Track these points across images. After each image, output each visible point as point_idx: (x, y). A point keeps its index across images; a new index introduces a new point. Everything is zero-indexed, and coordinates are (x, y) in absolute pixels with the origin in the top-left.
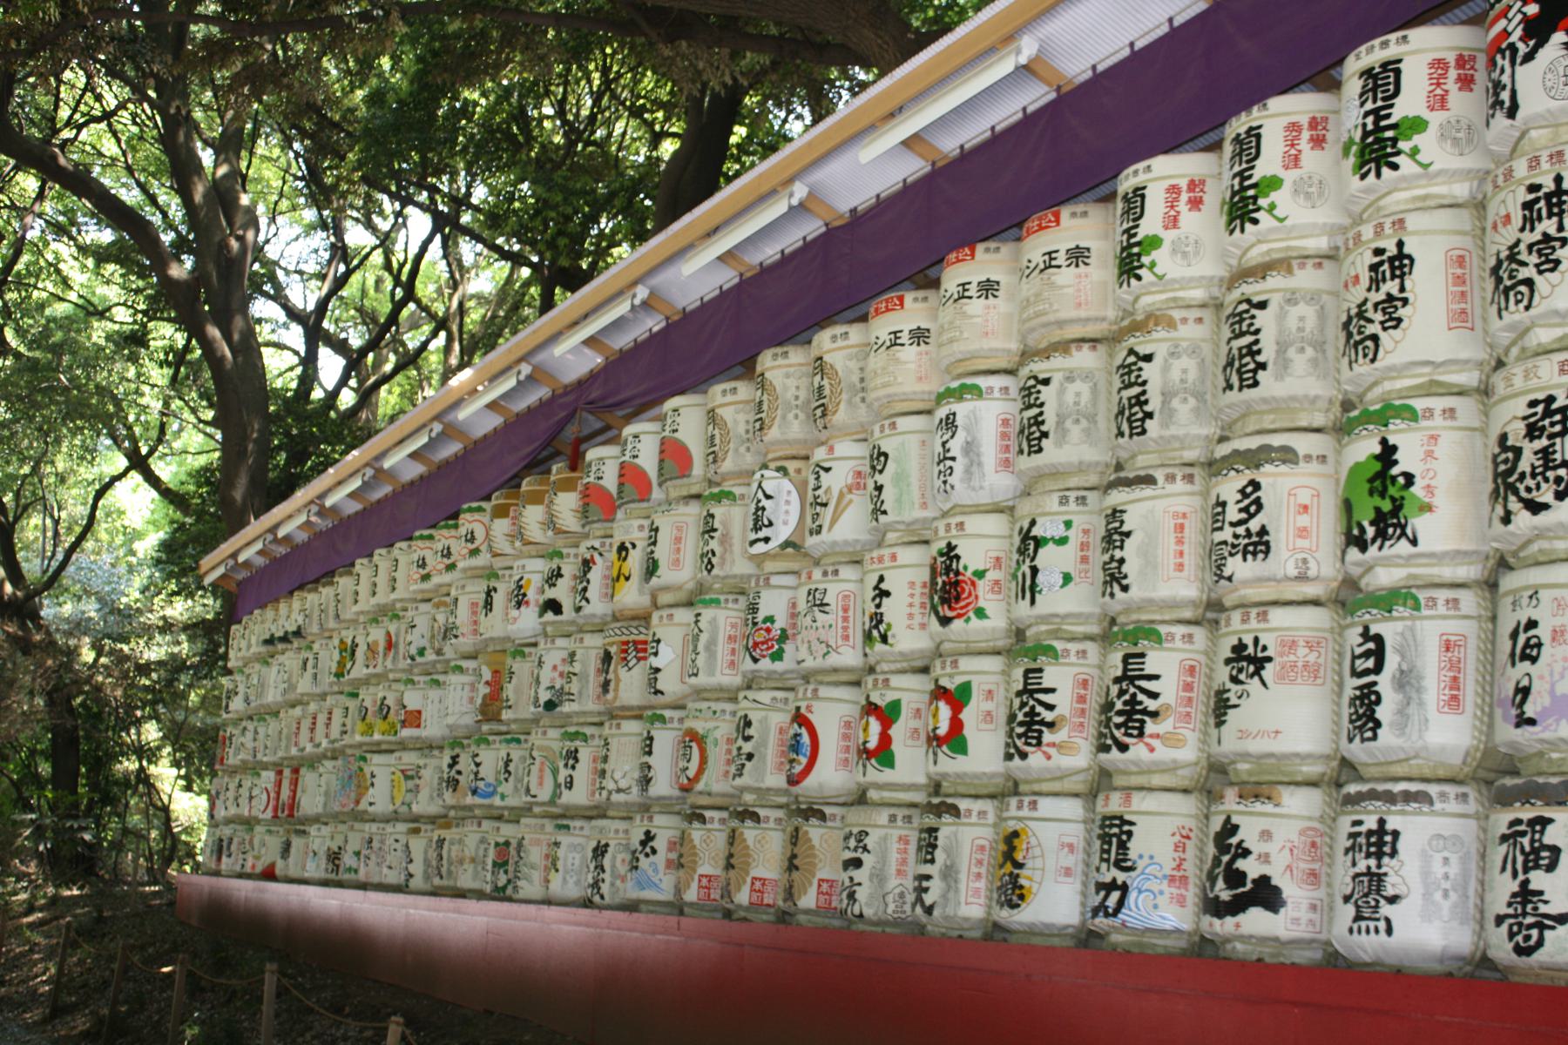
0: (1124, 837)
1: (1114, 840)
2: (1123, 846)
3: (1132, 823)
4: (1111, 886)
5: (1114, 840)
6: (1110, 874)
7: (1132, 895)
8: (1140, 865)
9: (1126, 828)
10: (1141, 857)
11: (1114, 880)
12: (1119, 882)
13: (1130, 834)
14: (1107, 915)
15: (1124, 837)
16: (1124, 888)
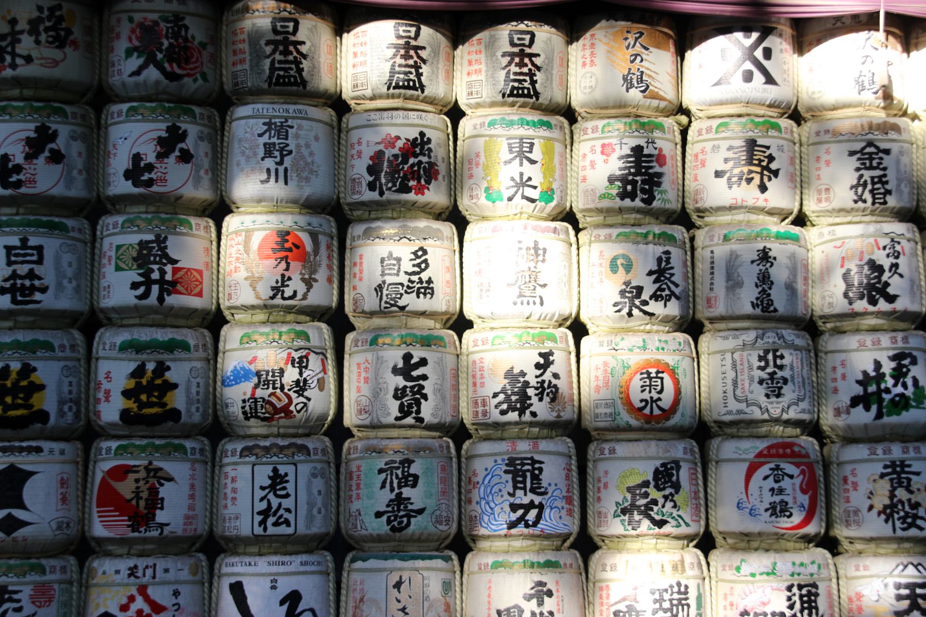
0: (537, 472)
1: (528, 474)
2: (536, 478)
5: (528, 474)
9: (537, 466)
11: (532, 501)
12: (537, 503)
14: (527, 526)
15: (537, 472)
16: (541, 507)
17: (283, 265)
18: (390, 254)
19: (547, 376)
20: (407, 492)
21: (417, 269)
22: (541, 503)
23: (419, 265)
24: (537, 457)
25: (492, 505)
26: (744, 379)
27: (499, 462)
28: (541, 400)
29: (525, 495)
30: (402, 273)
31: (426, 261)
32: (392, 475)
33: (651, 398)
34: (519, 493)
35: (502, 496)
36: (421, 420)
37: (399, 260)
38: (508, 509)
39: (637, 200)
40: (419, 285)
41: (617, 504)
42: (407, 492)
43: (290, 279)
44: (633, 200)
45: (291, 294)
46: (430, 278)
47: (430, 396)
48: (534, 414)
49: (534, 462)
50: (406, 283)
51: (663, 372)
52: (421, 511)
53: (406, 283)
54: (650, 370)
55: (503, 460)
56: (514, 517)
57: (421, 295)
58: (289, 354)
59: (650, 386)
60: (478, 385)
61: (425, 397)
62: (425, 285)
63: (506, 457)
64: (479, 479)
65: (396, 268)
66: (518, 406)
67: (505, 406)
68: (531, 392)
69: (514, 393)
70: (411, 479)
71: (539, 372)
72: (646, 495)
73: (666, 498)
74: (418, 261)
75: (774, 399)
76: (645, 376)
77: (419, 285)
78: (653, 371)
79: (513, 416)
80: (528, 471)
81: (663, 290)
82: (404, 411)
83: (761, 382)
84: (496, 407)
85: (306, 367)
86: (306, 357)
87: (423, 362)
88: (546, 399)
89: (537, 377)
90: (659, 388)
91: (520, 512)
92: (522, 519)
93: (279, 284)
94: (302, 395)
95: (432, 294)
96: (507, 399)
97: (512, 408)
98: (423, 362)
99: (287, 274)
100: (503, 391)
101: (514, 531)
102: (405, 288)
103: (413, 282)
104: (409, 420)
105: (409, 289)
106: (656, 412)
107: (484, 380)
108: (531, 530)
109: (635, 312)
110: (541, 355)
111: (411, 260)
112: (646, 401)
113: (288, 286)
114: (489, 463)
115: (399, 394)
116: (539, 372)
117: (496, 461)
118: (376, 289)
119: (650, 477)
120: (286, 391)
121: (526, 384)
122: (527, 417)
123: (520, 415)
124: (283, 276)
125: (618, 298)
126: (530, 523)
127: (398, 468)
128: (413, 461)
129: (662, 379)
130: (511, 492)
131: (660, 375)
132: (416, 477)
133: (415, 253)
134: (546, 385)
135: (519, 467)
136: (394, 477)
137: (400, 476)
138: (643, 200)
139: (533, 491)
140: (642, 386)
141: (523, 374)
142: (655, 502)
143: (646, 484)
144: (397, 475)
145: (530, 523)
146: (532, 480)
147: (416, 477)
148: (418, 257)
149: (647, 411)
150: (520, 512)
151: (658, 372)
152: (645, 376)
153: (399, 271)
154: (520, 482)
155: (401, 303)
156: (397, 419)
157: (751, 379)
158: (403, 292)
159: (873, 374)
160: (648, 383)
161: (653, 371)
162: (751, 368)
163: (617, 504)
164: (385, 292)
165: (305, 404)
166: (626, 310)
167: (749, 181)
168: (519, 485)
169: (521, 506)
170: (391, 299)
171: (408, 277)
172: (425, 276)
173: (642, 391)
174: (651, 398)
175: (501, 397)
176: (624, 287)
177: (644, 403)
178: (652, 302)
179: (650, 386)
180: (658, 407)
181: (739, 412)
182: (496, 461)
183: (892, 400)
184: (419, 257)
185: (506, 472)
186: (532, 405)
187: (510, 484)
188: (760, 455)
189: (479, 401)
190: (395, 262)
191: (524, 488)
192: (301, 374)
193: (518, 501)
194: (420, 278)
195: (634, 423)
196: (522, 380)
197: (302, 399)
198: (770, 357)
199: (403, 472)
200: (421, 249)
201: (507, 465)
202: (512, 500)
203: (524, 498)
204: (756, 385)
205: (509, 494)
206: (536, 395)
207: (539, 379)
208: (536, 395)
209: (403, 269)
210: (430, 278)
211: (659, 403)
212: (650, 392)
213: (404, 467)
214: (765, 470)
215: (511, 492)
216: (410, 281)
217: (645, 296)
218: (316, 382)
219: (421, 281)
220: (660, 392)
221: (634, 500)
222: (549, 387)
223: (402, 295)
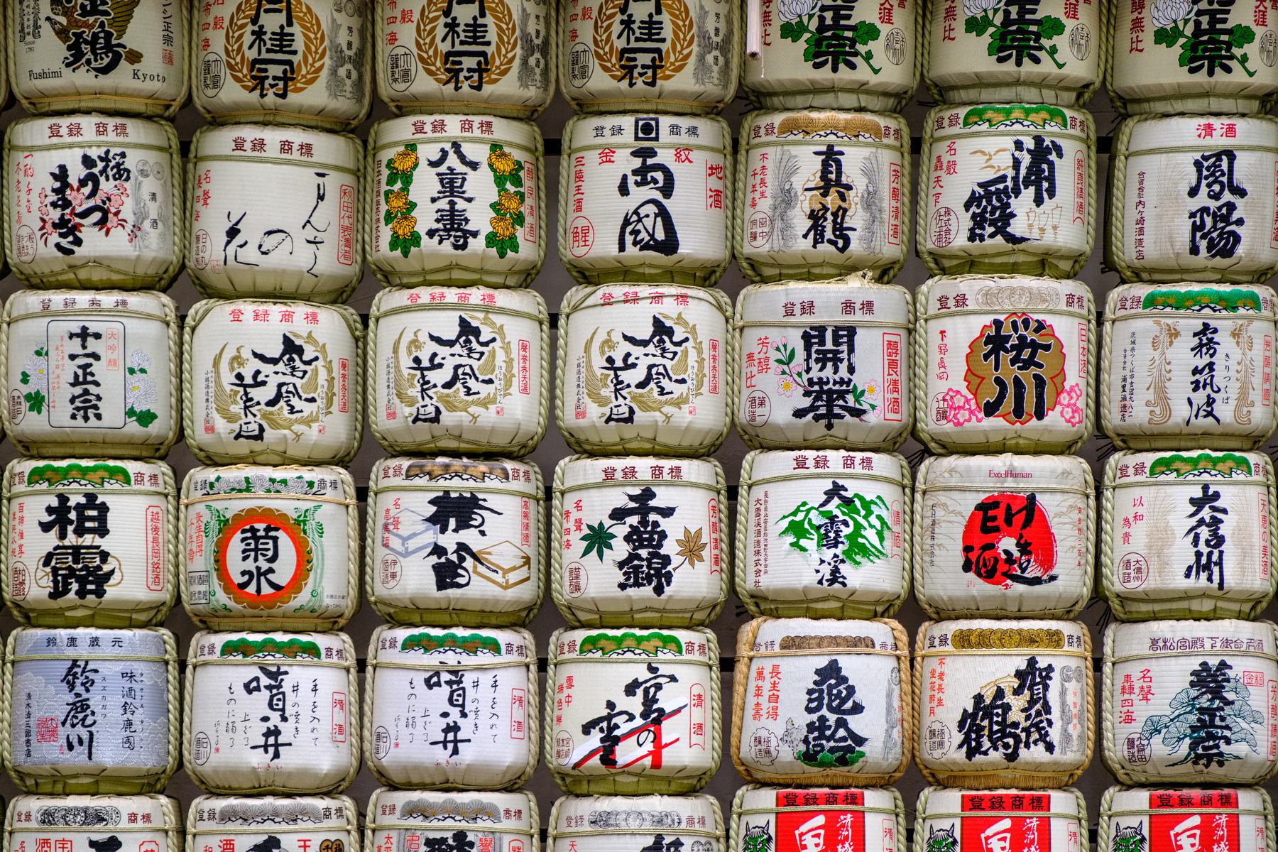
33: (258, 568)
51: (277, 529)
54: (257, 526)
59: (256, 550)
76: (249, 535)
78: (261, 526)
90: (270, 553)
106: (266, 590)
129: (275, 539)
131: (272, 534)
140: (244, 551)
149: (252, 589)
151: (268, 529)
152: (249, 535)
160: (252, 546)
161: (261, 526)
173: (245, 559)
174: (258, 568)
177: (246, 577)
179: (256, 550)
180: (268, 580)
211: (270, 576)
212: (256, 560)
220: (274, 558)
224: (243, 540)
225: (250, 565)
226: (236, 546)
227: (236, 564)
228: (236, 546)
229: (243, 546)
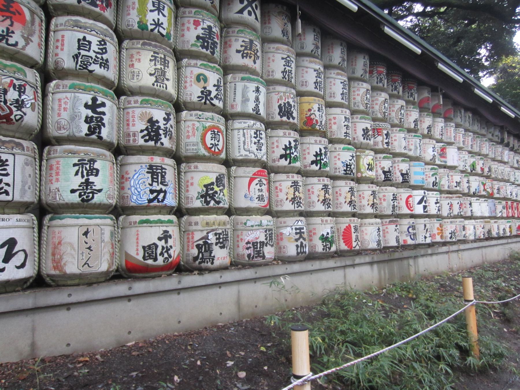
1: (160, 174)
2: (163, 177)
3: (165, 169)
4: (160, 191)
5: (160, 174)
6: (156, 187)
7: (168, 195)
8: (169, 184)
9: (164, 170)
10: (169, 181)
11: (161, 189)
12: (163, 190)
13: (165, 173)
14: (158, 202)
15: (163, 174)
16: (165, 192)
17: (8, 22)
18: (84, 37)
19: (168, 126)
20: (92, 179)
21: (100, 51)
22: (165, 190)
23: (101, 49)
24: (164, 166)
25: (139, 190)
26: (248, 140)
27: (144, 166)
28: (165, 137)
29: (158, 185)
30: (91, 51)
31: (105, 48)
32: (82, 168)
34: (155, 184)
35: (145, 185)
36: (100, 138)
37: (90, 43)
38: (149, 192)
39: (209, 51)
40: (101, 61)
41: (199, 193)
42: (92, 179)
43: (13, 32)
44: (207, 50)
45: (14, 43)
46: (107, 59)
47: (106, 125)
48: (162, 144)
49: (162, 168)
50: (94, 57)
52: (100, 191)
53: (94, 57)
55: (146, 166)
56: (152, 196)
57: (102, 67)
58: (12, 81)
59: (215, 137)
60: (131, 125)
61: (104, 125)
62: (104, 62)
63: (148, 165)
64: (131, 175)
65: (88, 47)
66: (155, 138)
67: (147, 138)
68: (161, 132)
69: (152, 131)
70: (94, 171)
71: (165, 123)
72: (212, 189)
73: (220, 190)
74: (101, 47)
75: (259, 151)
77: (101, 61)
79: (152, 143)
80: (159, 173)
81: (219, 95)
82: (91, 131)
83: (255, 143)
84: (142, 137)
85: (24, 92)
86: (24, 86)
87: (103, 105)
88: (168, 137)
89: (164, 125)
91: (155, 194)
92: (156, 198)
93: (5, 34)
94: (21, 111)
95: (108, 68)
96: (149, 134)
97: (151, 139)
98: (103, 105)
99: (11, 29)
100: (147, 129)
101: (152, 204)
102: (93, 60)
103: (98, 58)
104: (94, 137)
105: (95, 62)
106: (217, 150)
107: (135, 123)
108: (160, 204)
109: (208, 102)
110: (166, 113)
111: (97, 45)
112: (213, 144)
113: (11, 37)
114: (137, 167)
115: (88, 120)
116: (165, 123)
117: (141, 166)
118: (73, 57)
119: (214, 181)
120: (8, 104)
121: (159, 127)
122: (159, 144)
123: (155, 143)
124: (8, 29)
125: (200, 95)
126: (160, 200)
127: (87, 164)
128: (96, 161)
130: (151, 183)
132: (98, 171)
133: (100, 42)
134: (168, 130)
135: (155, 170)
136: (84, 169)
137: (88, 169)
138: (211, 52)
139: (162, 183)
141: (157, 122)
142: (216, 192)
143: (212, 184)
144: (86, 169)
145: (160, 200)
146: (161, 178)
147: (98, 171)
148: (101, 45)
149: (213, 149)
150: (155, 194)
153: (90, 49)
154: (155, 178)
155: (90, 68)
156: (86, 135)
157: (251, 141)
158: (92, 62)
159: (288, 146)
161: (216, 131)
162: (251, 137)
163: (199, 193)
164: (80, 60)
165: (22, 117)
166: (204, 101)
167: (250, 57)
168: (155, 180)
169: (155, 191)
170: (84, 64)
171: (95, 54)
172: (105, 56)
173: (212, 140)
175: (146, 132)
176: (203, 89)
177: (212, 146)
178: (215, 99)
181: (246, 155)
182: (141, 166)
183: (294, 157)
184: (102, 45)
185: (148, 172)
186: (161, 139)
187: (150, 179)
188: (254, 174)
189: (131, 134)
190: (87, 43)
191: (157, 182)
192: (20, 96)
193: (154, 188)
194: (102, 57)
195: (207, 154)
196: (157, 125)
197: (19, 112)
198: (258, 133)
199: (90, 167)
200: (103, 40)
201: (148, 169)
202: (151, 187)
203: (157, 187)
204: (253, 144)
205: (149, 184)
206: (164, 134)
207: (165, 126)
208: (164, 134)
209: (92, 48)
210: (107, 59)
213: (90, 164)
214: (256, 181)
215: (151, 183)
216: (96, 56)
217: (212, 95)
218: (30, 104)
219: (102, 59)
221: (207, 191)
222: (169, 131)
223: (91, 63)
224: (211, 134)
225: (213, 142)
226: (209, 135)
227: (209, 141)
228: (209, 135)
229: (211, 136)
